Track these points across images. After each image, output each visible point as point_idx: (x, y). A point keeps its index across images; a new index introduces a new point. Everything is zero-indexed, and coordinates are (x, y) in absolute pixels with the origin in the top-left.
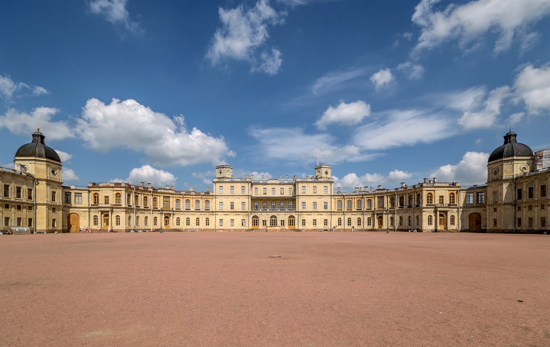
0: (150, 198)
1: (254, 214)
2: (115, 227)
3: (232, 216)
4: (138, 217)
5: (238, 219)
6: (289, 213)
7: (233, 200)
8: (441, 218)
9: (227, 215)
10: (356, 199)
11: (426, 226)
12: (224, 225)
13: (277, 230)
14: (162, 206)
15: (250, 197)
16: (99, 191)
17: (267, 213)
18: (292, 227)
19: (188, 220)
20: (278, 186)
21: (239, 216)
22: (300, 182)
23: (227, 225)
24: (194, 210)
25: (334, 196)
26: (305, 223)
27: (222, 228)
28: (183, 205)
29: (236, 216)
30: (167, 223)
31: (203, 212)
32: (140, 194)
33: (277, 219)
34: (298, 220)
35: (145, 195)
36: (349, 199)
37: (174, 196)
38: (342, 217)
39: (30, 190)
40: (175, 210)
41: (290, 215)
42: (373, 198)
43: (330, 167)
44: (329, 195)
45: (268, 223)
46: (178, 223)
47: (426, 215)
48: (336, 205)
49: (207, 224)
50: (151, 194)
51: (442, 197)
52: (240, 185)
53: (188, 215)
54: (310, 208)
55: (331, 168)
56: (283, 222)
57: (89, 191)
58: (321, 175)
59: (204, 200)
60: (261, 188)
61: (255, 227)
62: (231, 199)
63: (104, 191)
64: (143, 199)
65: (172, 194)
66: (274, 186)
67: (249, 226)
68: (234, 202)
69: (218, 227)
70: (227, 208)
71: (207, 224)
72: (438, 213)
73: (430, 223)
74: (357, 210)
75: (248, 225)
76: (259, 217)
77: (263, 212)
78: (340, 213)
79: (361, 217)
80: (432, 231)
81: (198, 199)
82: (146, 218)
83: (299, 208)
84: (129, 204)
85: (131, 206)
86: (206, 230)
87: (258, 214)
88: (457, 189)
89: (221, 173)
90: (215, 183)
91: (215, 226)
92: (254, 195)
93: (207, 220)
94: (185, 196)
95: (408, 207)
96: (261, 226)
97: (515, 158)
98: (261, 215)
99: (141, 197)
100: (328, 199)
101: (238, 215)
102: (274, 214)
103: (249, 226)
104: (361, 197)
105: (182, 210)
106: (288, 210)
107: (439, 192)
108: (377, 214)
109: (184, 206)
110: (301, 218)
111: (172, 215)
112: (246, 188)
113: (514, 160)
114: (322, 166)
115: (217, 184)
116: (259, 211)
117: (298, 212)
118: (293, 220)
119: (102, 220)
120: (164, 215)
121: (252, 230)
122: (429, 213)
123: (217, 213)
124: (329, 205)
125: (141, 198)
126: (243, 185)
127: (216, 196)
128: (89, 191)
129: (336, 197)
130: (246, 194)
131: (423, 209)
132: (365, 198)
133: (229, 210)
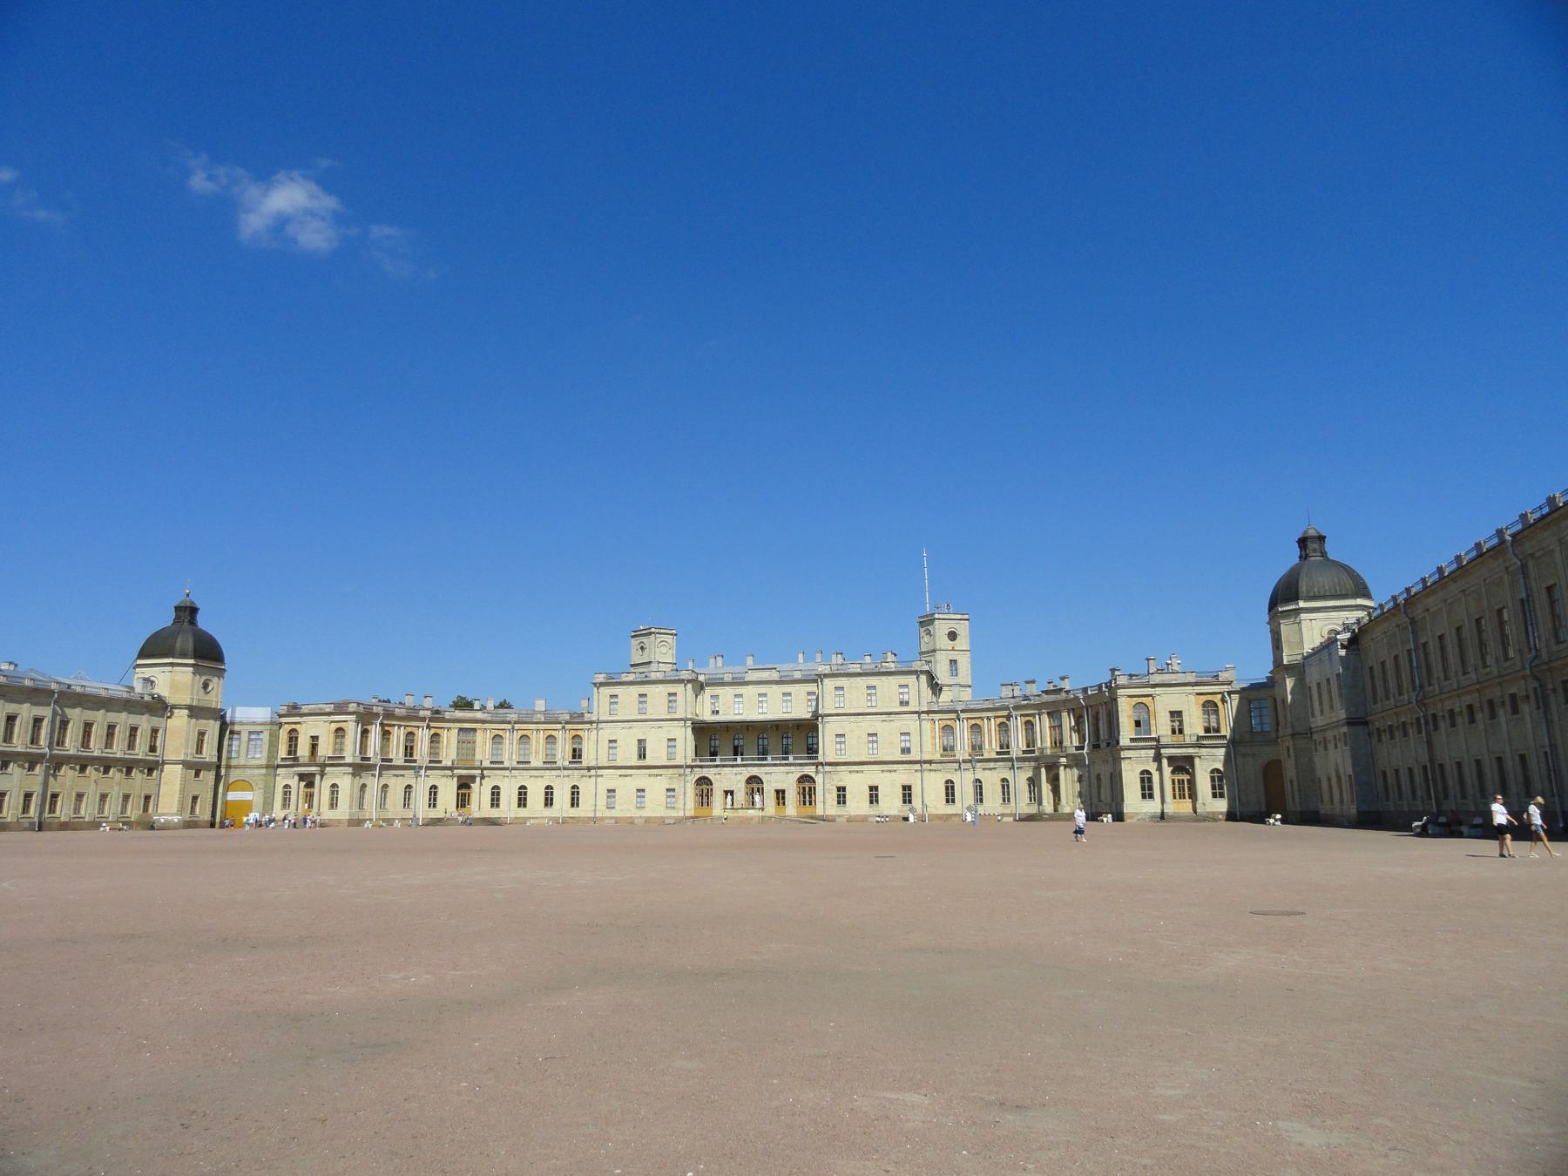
0: (423, 737)
1: (699, 773)
2: (327, 814)
3: (641, 779)
4: (385, 786)
5: (656, 786)
6: (798, 768)
7: (644, 733)
8: (1177, 777)
9: (626, 776)
10: (992, 719)
11: (1132, 800)
12: (617, 807)
13: (751, 819)
14: (453, 755)
15: (689, 723)
16: (299, 723)
17: (735, 769)
18: (808, 810)
19: (523, 792)
20: (775, 687)
22: (826, 676)
23: (625, 807)
25: (928, 712)
26: (844, 796)
27: (613, 813)
28: (510, 753)
30: (463, 801)
31: (565, 769)
32: (396, 728)
33: (765, 785)
34: (824, 787)
35: (409, 729)
36: (973, 722)
37: (487, 726)
38: (956, 778)
39: (155, 731)
40: (489, 766)
41: (802, 773)
42: (1037, 717)
43: (966, 617)
44: (913, 709)
45: (740, 796)
46: (495, 799)
47: (1133, 771)
48: (937, 740)
49: (574, 802)
50: (425, 725)
51: (1176, 715)
52: (662, 690)
53: (523, 778)
54: (857, 749)
55: (968, 620)
56: (780, 795)
58: (935, 643)
59: (569, 735)
60: (726, 693)
61: (704, 811)
62: (639, 732)
64: (402, 738)
65: (484, 722)
66: (763, 689)
67: (684, 810)
69: (603, 811)
70: (628, 755)
71: (574, 802)
72: (1165, 762)
73: (1147, 792)
74: (998, 753)
75: (682, 807)
76: (713, 781)
77: (724, 766)
78: (950, 765)
79: (1008, 775)
80: (1152, 817)
81: (553, 733)
82: (433, 790)
83: (827, 752)
84: (365, 753)
85: (369, 759)
86: (571, 820)
87: (709, 773)
88: (1226, 688)
90: (598, 688)
91: (593, 808)
92: (708, 717)
93: (575, 791)
94: (517, 726)
95: (1108, 744)
96: (718, 807)
97: (1302, 604)
98: (718, 776)
99: (398, 735)
100: (911, 723)
101: (657, 775)
102: (754, 771)
103: (684, 810)
104: (1005, 713)
105: (506, 764)
106: (795, 758)
107: (1165, 702)
108: (1171, 759)
109: (514, 752)
110: (834, 783)
111: (478, 779)
112: (680, 698)
113: (1298, 611)
114: (936, 616)
115: (602, 689)
117: (821, 764)
118: (810, 788)
119: (300, 796)
120: (455, 779)
122: (1142, 763)
123: (600, 772)
124: (915, 738)
125: (398, 737)
126: (672, 688)
127: (598, 722)
129: (937, 716)
131: (1122, 753)
132: (1016, 718)
133: (635, 761)
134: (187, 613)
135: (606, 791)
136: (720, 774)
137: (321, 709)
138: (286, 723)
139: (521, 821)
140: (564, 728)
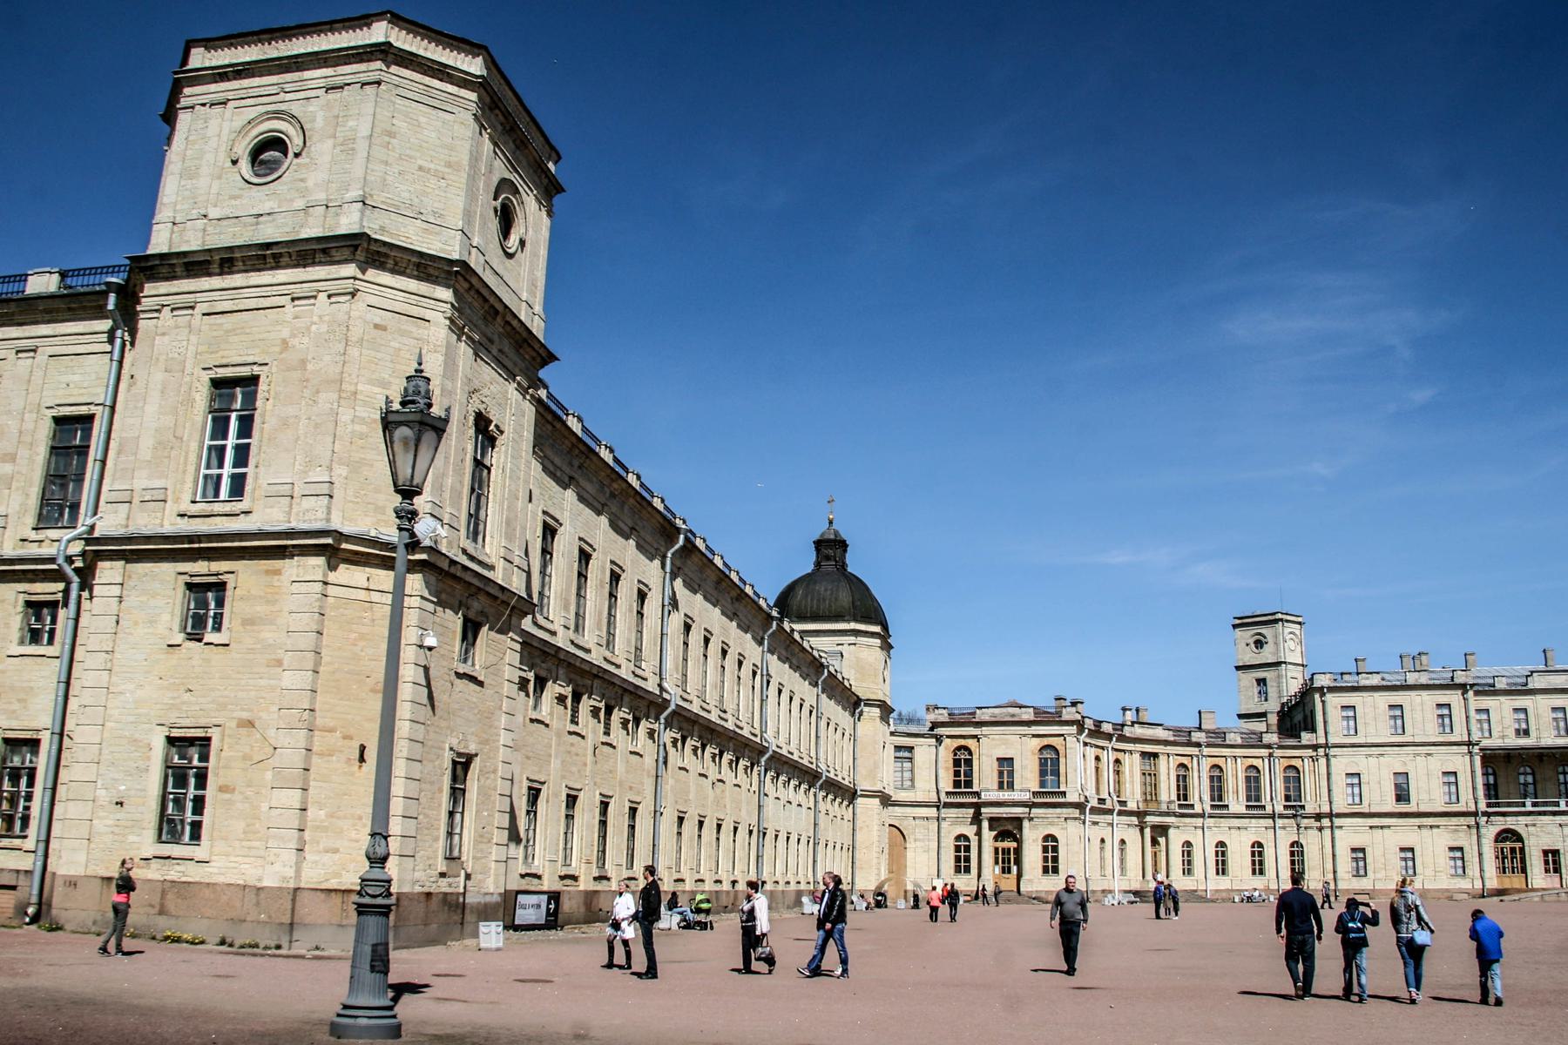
5: (1433, 845)
9: (1382, 827)
15: (1476, 749)
17: (1558, 818)
21: (1435, 830)
24: (1243, 810)
29: (1425, 832)
31: (1281, 816)
37: (1170, 749)
52: (1429, 699)
57: (939, 739)
60: (1501, 708)
62: (1395, 761)
63: (993, 739)
65: (1166, 743)
68: (1012, 759)
70: (1381, 797)
76: (1524, 835)
77: (1540, 813)
87: (1518, 824)
89: (1259, 644)
98: (1530, 828)
105: (1198, 809)
116: (1523, 809)
121: (1500, 892)
123: (1337, 822)
128: (939, 739)
130: (1459, 734)
133: (1390, 805)
134: (831, 548)
135: (1349, 851)
136: (1534, 825)
137: (1013, 716)
138: (948, 737)
139: (1224, 895)
140: (1271, 755)
